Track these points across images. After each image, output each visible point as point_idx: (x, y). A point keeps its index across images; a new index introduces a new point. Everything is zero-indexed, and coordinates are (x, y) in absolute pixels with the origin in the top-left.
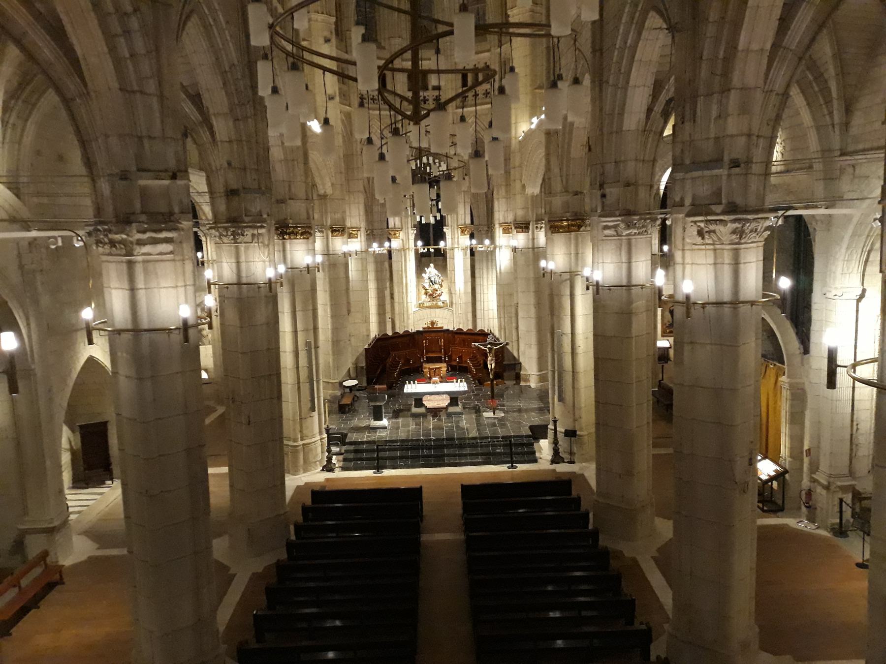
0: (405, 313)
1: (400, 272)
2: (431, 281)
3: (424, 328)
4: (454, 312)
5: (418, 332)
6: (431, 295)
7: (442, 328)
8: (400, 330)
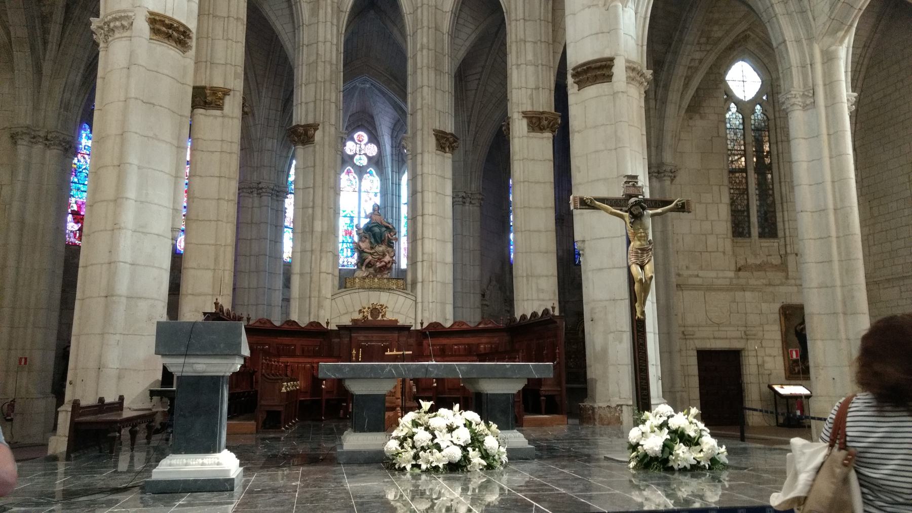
0: (315, 293)
1: (310, 211)
2: (374, 235)
3: (353, 321)
4: (419, 300)
5: (342, 328)
6: (369, 265)
7: (396, 321)
8: (299, 316)
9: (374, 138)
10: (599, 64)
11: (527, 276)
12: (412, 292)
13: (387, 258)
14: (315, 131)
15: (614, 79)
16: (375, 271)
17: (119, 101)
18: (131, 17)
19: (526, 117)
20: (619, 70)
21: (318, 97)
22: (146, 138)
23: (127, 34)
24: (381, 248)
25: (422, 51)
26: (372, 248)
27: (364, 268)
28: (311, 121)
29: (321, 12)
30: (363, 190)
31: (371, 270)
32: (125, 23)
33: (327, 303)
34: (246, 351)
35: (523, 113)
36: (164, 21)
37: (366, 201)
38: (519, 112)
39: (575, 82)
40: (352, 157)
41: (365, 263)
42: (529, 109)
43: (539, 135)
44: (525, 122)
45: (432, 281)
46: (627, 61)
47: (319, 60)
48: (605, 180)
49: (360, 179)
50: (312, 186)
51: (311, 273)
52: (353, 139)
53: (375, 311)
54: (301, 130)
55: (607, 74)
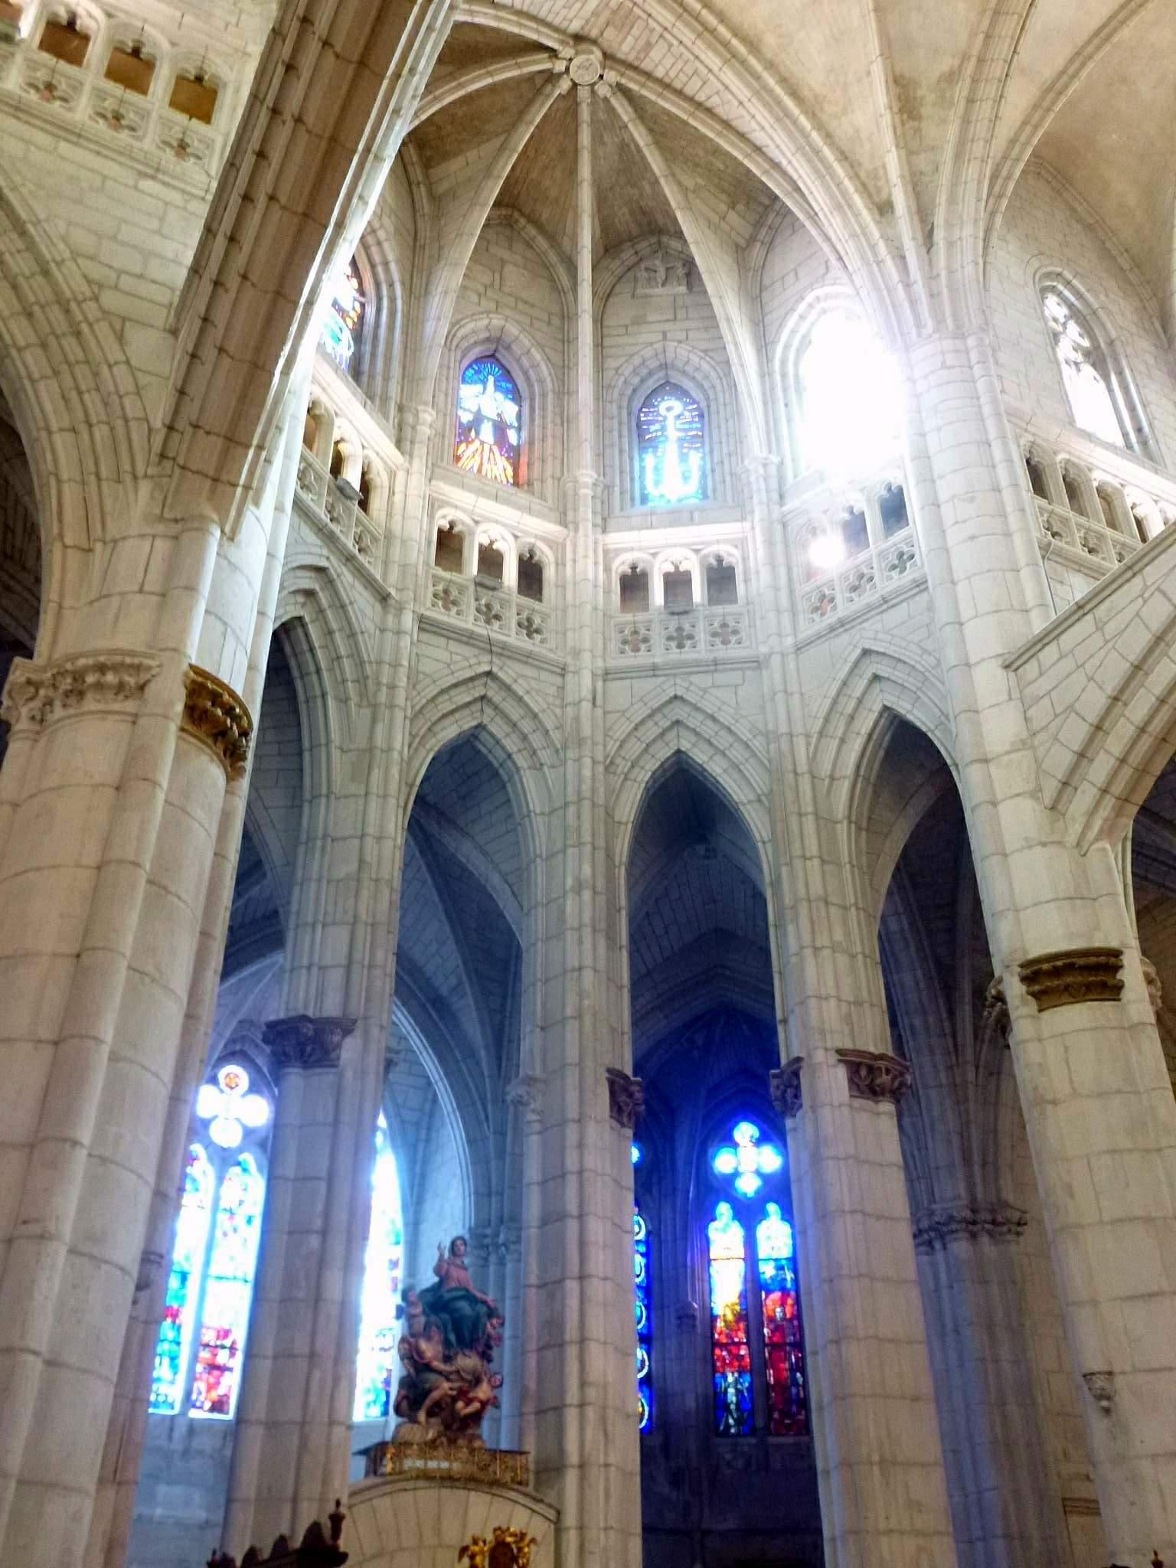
1: (314, 1241)
2: (457, 1324)
4: (570, 1519)
10: (1093, 960)
11: (882, 1462)
12: (536, 1489)
14: (344, 1037)
15: (1127, 994)
16: (447, 1426)
17: (78, 866)
18: (149, 668)
19: (846, 1062)
21: (357, 956)
22: (137, 975)
23: (130, 706)
24: (468, 1361)
25: (579, 894)
26: (447, 1359)
27: (422, 1416)
29: (376, 774)
30: (223, 1204)
32: (131, 680)
35: (839, 1052)
36: (221, 696)
37: (225, 1234)
38: (826, 1049)
39: (1034, 995)
40: (206, 1124)
41: (428, 1402)
42: (848, 1045)
43: (870, 1104)
44: (841, 1074)
45: (607, 1465)
47: (365, 876)
48: (1148, 1220)
50: (324, 1174)
51: (303, 1424)
52: (213, 1080)
54: (309, 1030)
55: (1111, 982)
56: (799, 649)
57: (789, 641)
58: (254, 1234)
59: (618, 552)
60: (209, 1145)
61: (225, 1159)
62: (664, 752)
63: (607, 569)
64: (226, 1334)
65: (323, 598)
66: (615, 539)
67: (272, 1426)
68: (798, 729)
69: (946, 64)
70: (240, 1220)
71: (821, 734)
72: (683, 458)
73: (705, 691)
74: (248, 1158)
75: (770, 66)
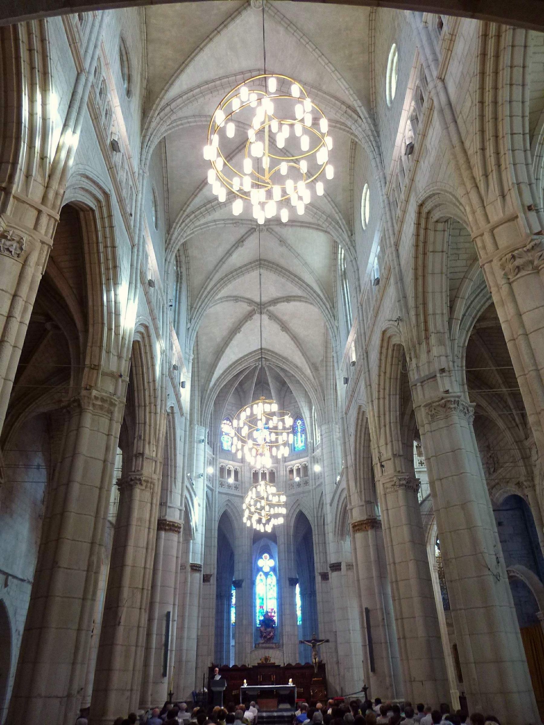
3: (258, 664)
5: (254, 667)
6: (265, 637)
7: (275, 663)
9: (271, 557)
13: (272, 634)
20: (343, 566)
23: (184, 571)
24: (269, 630)
26: (265, 630)
28: (241, 578)
31: (266, 639)
33: (249, 655)
34: (226, 685)
35: (320, 573)
40: (262, 568)
42: (322, 571)
46: (346, 563)
49: (267, 578)
52: (262, 558)
53: (266, 659)
56: (315, 489)
57: (314, 486)
58: (275, 589)
59: (288, 466)
60: (263, 572)
61: (266, 574)
62: (298, 510)
63: (286, 471)
64: (273, 609)
65: (230, 504)
66: (287, 464)
67: (239, 643)
68: (315, 507)
69: (320, 359)
70: (272, 586)
71: (319, 507)
72: (301, 436)
73: (302, 498)
74: (272, 573)
75: (291, 362)
